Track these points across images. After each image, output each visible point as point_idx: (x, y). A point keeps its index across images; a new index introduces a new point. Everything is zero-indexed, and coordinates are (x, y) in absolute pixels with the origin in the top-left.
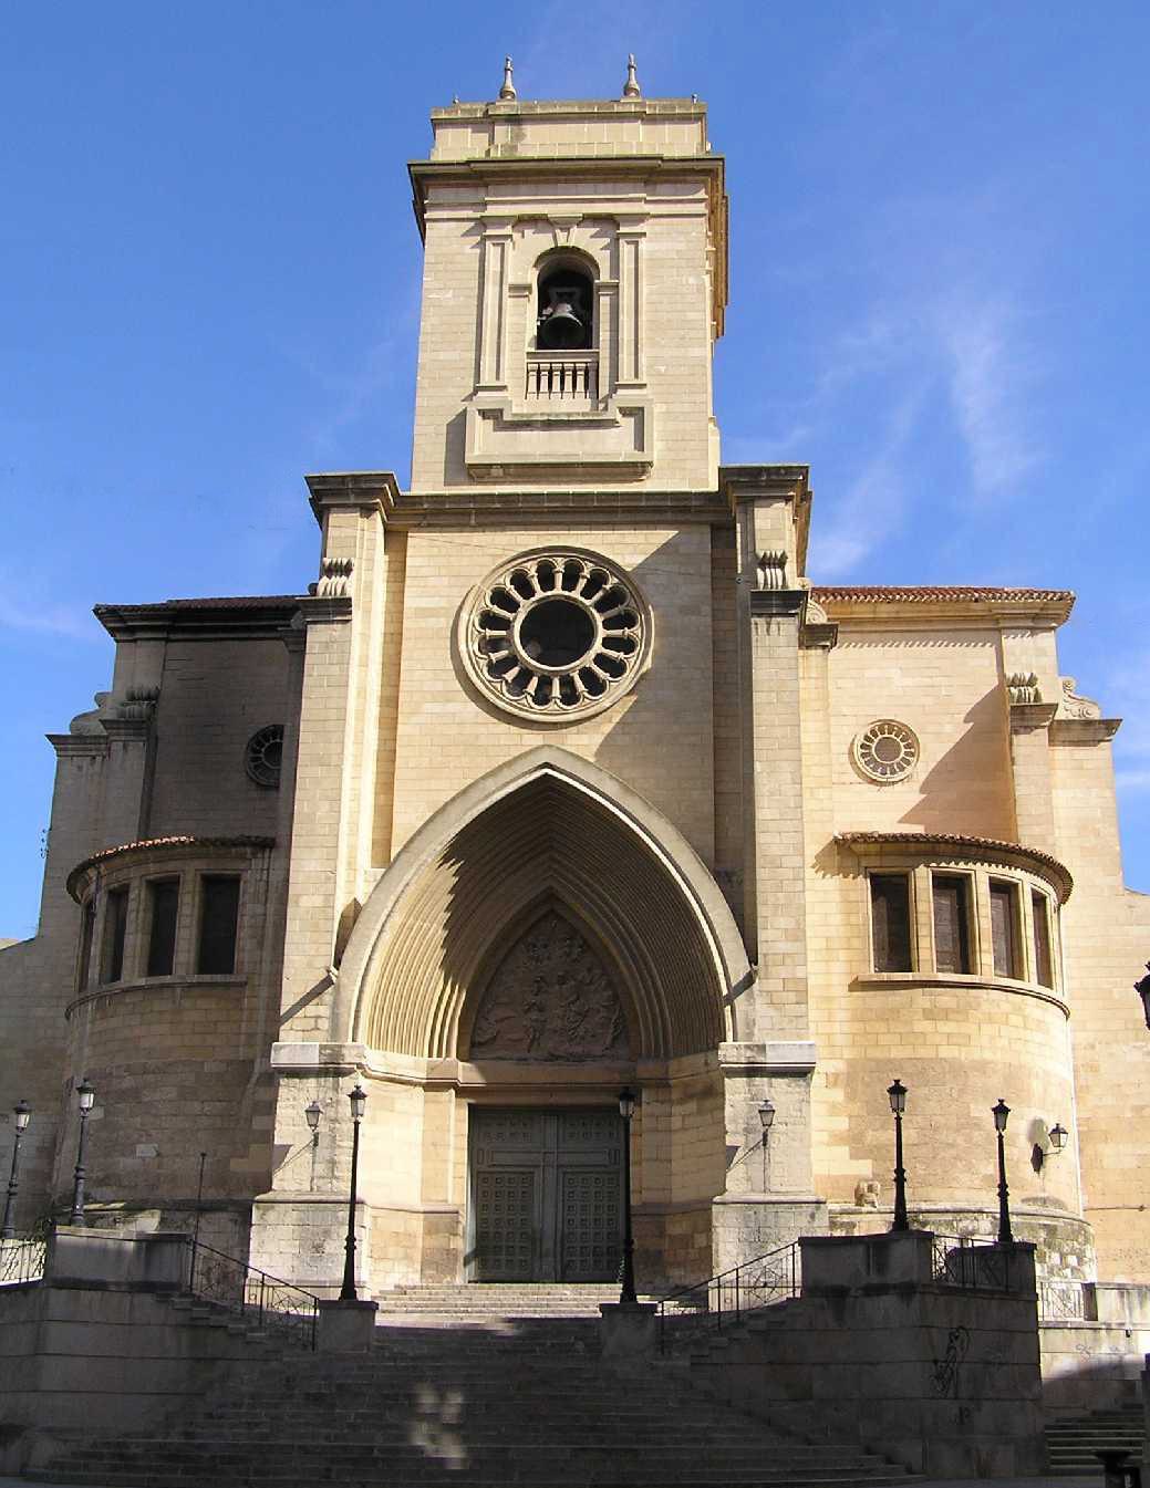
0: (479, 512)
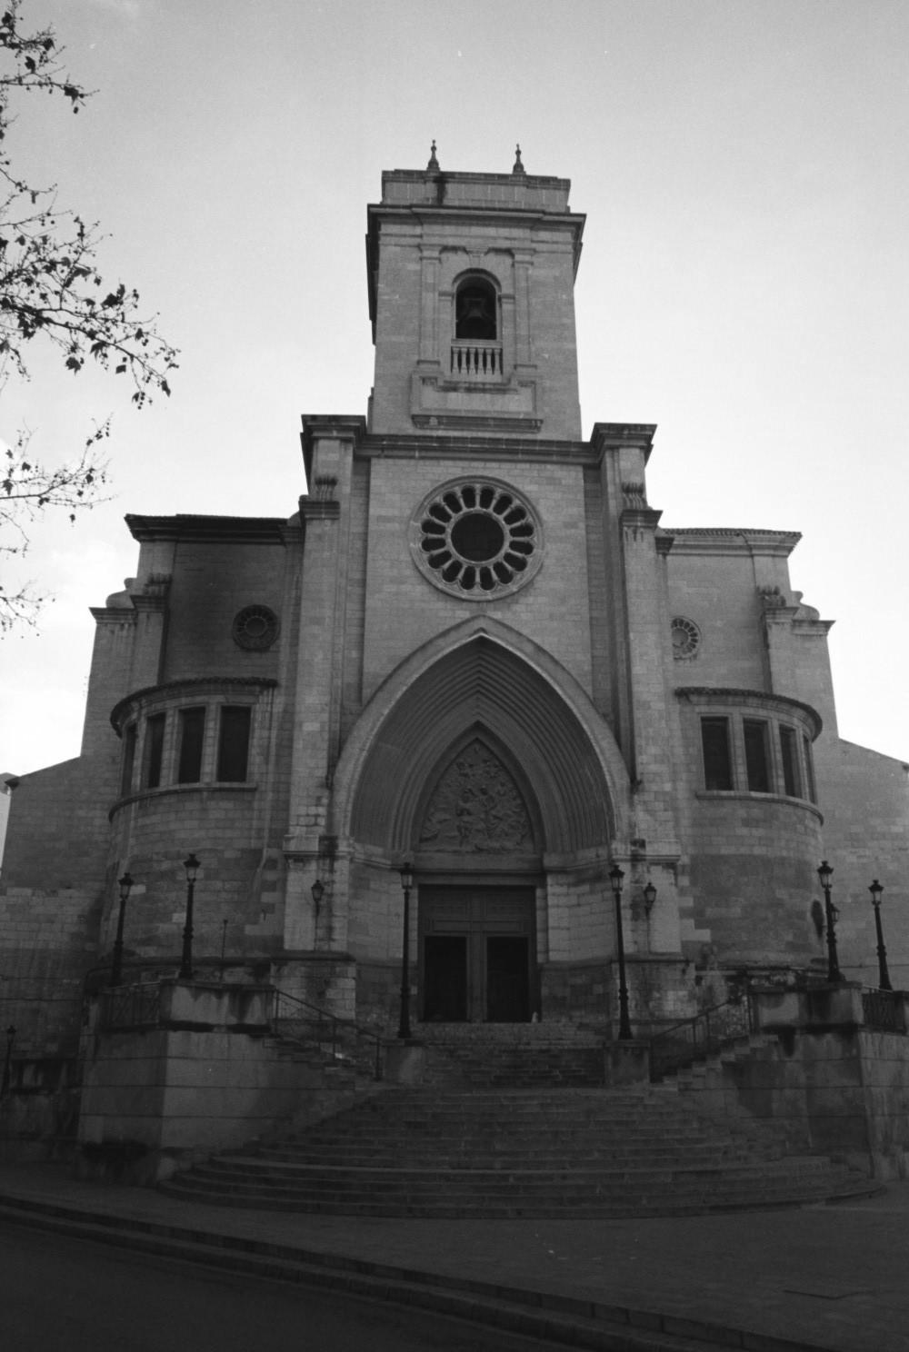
0: (421, 449)
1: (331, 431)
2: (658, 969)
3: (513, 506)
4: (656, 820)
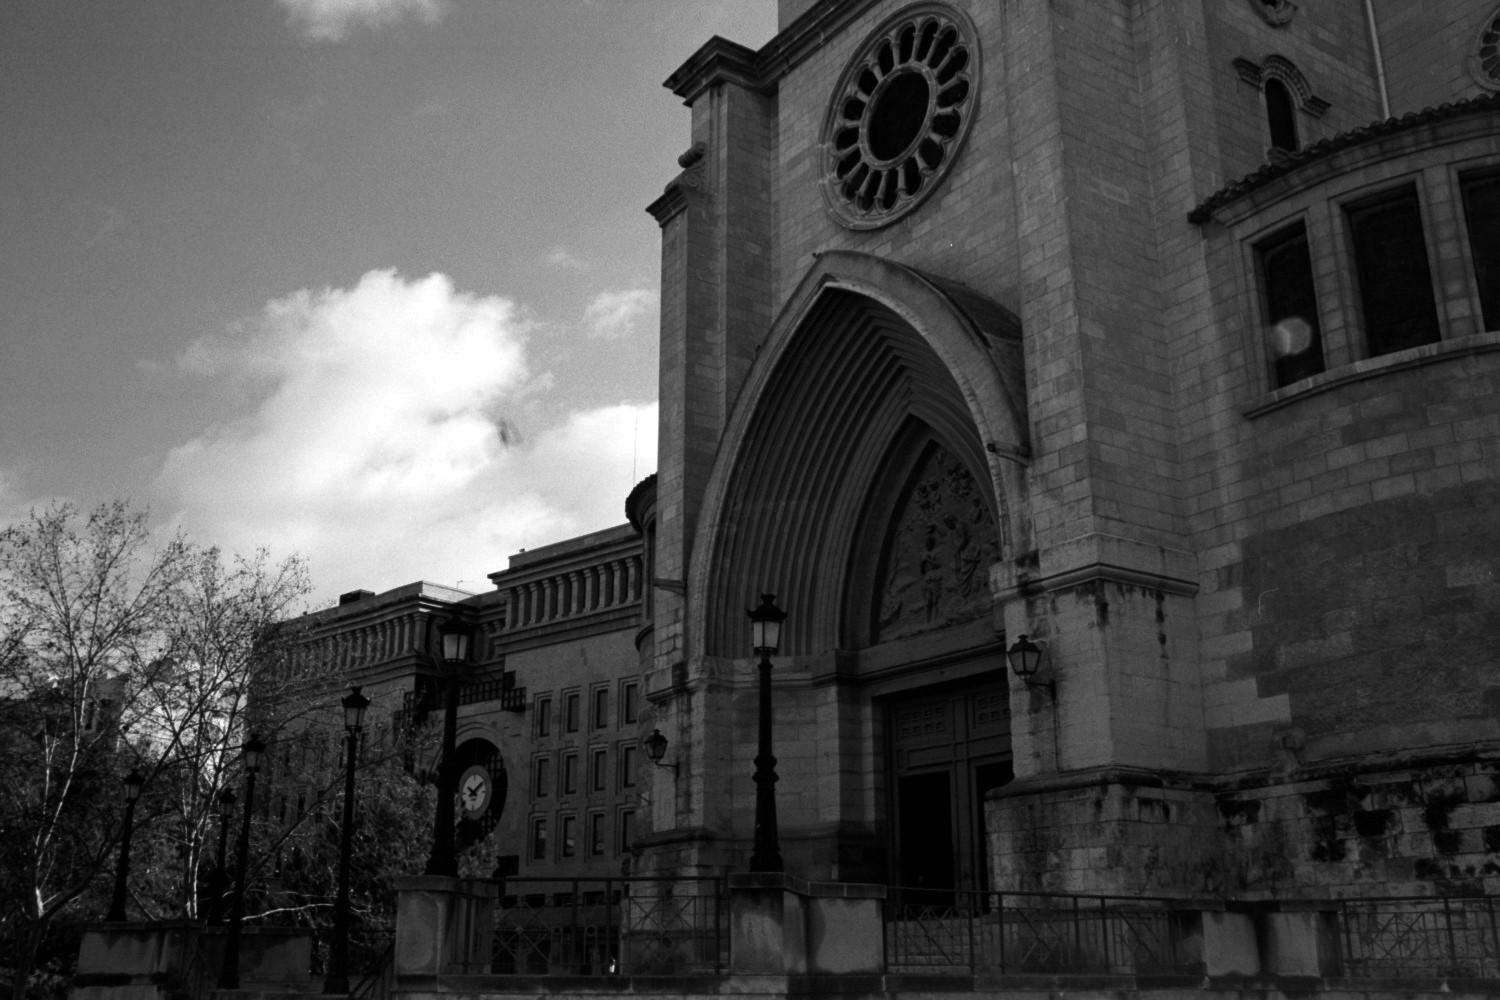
1: (698, 82)
2: (1054, 804)
3: (893, 42)
4: (1063, 505)
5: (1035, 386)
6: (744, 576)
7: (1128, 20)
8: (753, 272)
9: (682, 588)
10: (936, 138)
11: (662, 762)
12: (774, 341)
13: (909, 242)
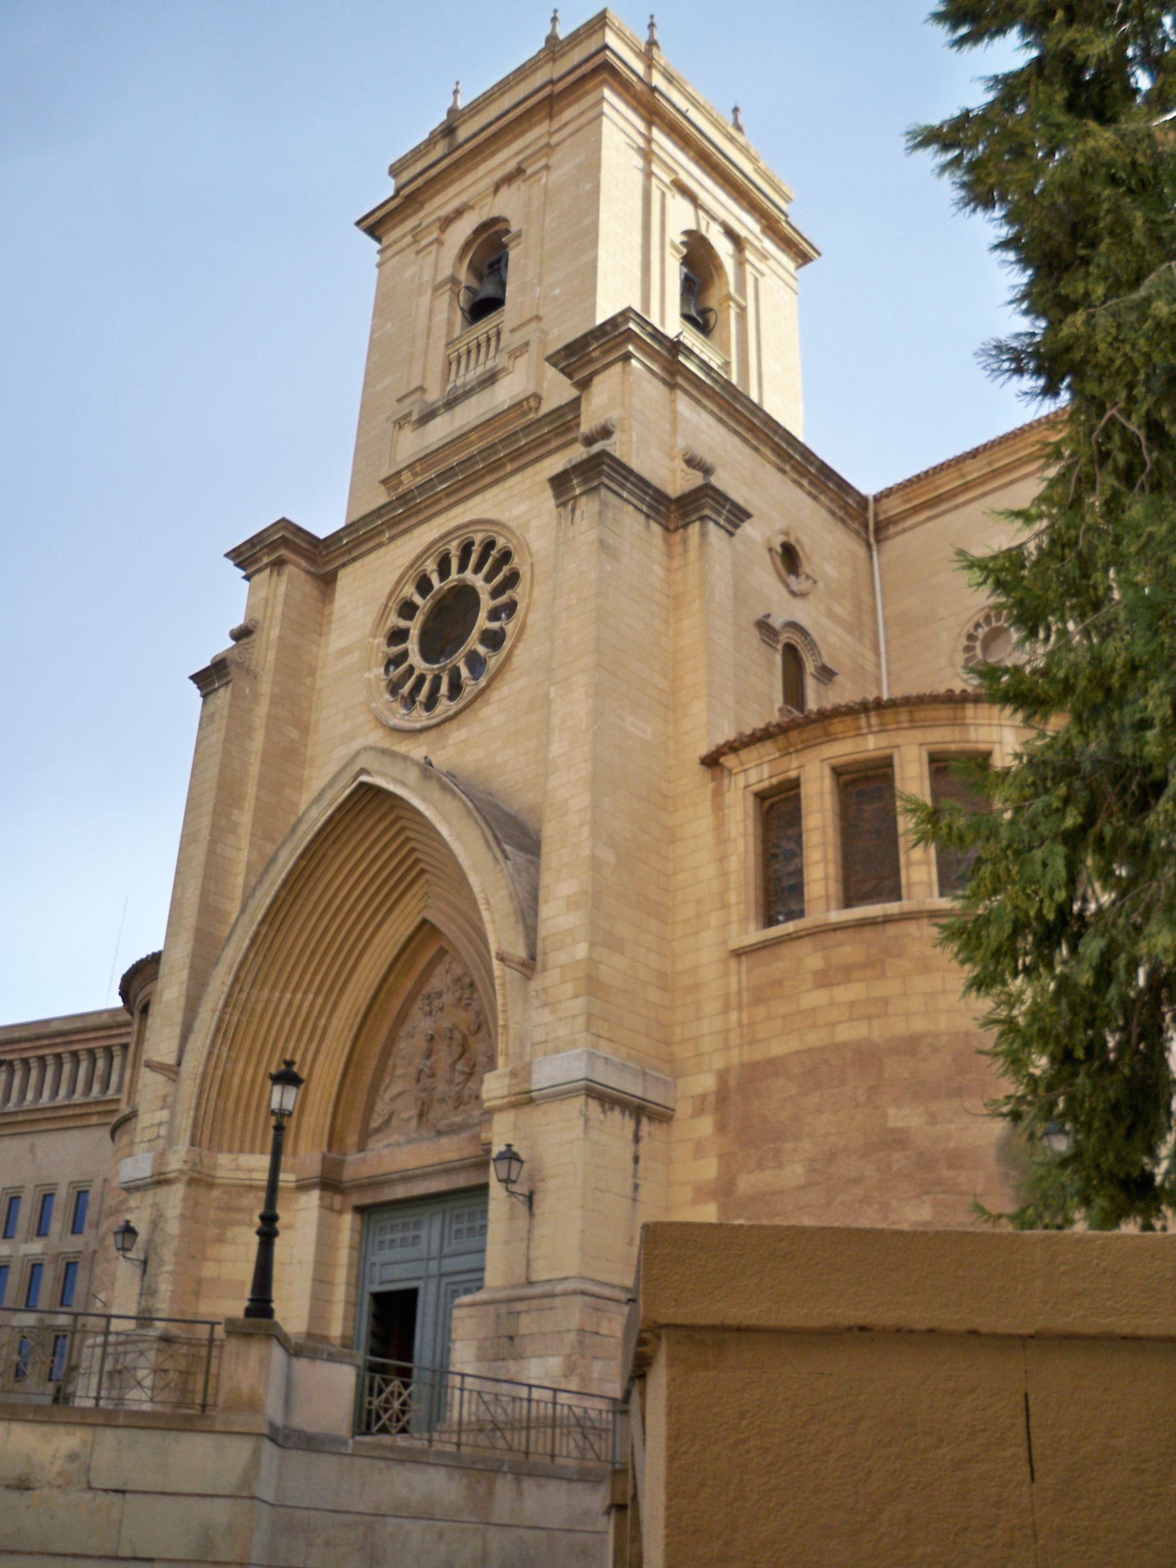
1: (260, 559)
5: (547, 902)
6: (241, 1065)
7: (669, 570)
8: (287, 757)
9: (172, 1072)
10: (482, 650)
11: (129, 1255)
12: (303, 828)
13: (444, 748)
